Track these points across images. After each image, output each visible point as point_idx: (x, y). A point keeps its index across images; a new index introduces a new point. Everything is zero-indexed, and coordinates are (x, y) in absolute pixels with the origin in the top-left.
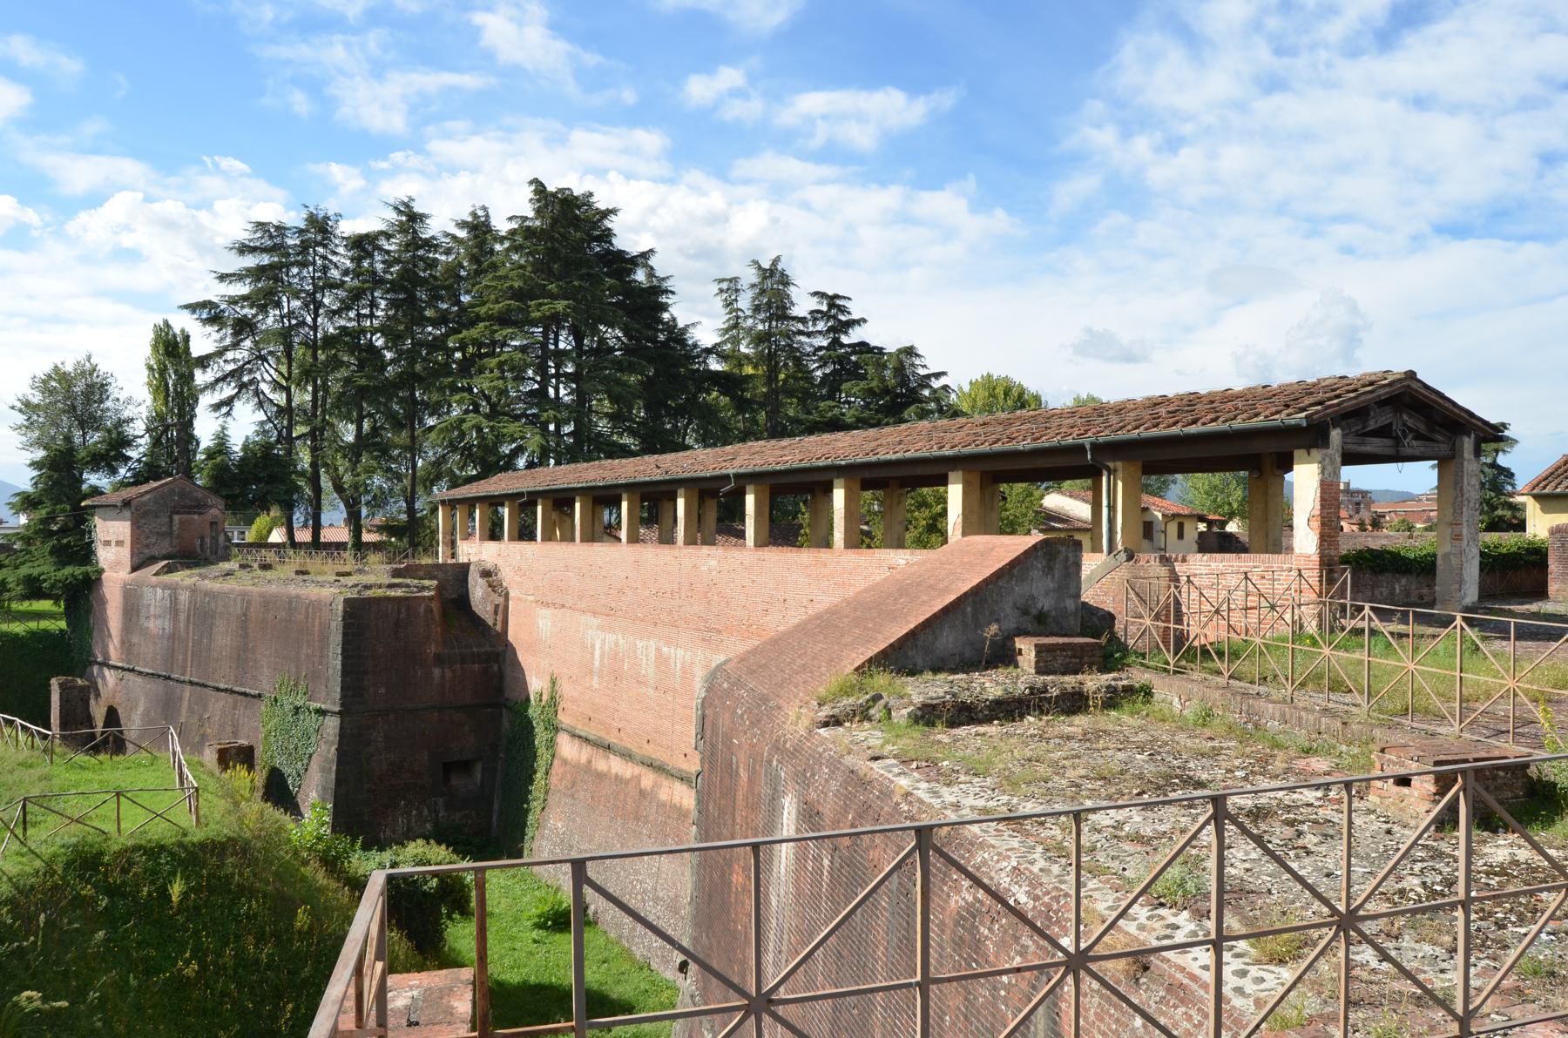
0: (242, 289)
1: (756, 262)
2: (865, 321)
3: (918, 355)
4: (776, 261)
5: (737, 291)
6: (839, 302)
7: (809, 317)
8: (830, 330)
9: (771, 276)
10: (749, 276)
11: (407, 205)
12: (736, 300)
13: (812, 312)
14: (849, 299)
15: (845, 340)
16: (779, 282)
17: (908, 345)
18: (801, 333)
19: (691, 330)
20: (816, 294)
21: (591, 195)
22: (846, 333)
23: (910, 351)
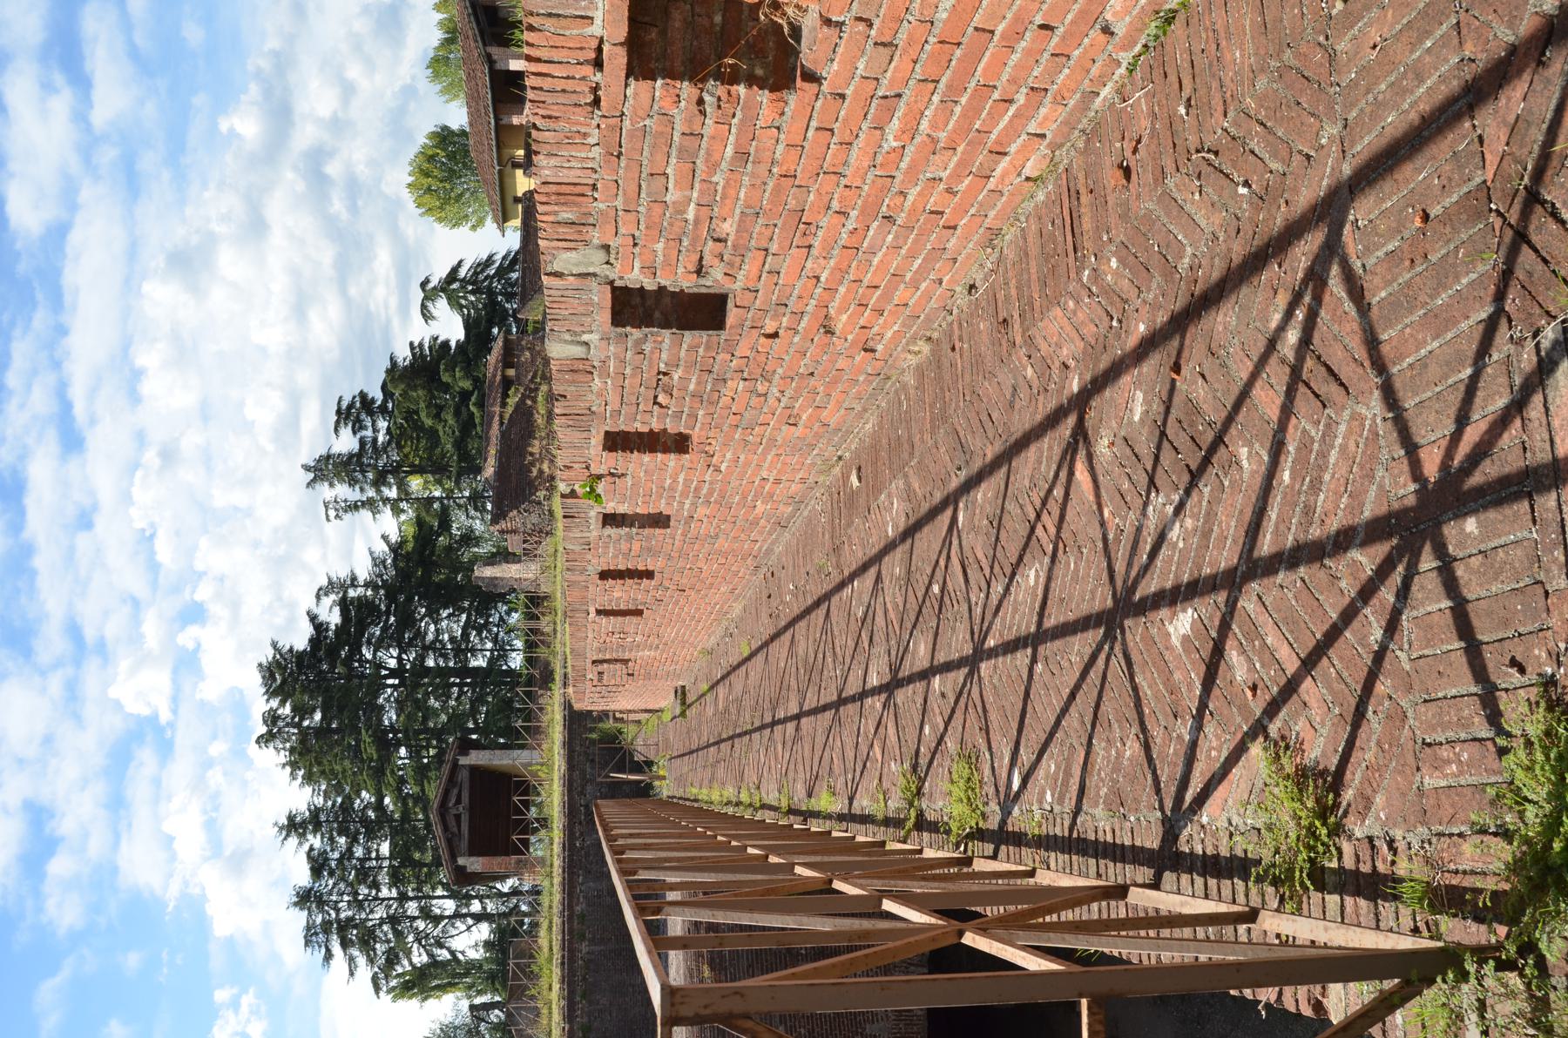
0: (361, 960)
1: (309, 485)
4: (307, 468)
6: (344, 407)
7: (358, 436)
8: (371, 413)
9: (321, 470)
10: (326, 492)
11: (281, 828)
12: (346, 501)
13: (354, 433)
16: (327, 464)
18: (375, 440)
19: (376, 555)
20: (336, 430)
21: (260, 665)
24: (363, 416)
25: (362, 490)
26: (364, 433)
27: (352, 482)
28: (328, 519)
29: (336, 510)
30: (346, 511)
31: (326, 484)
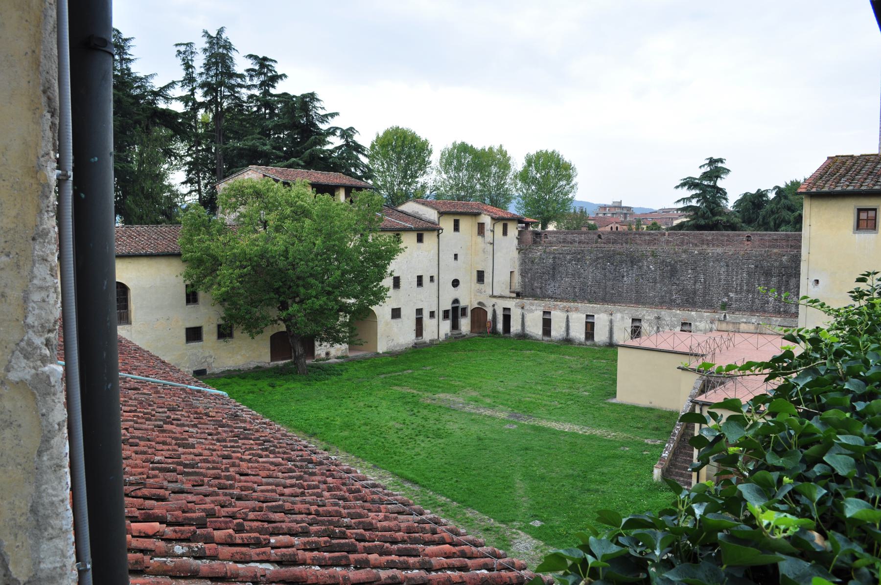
2: (285, 76)
3: (318, 100)
4: (220, 31)
5: (192, 53)
7: (246, 73)
8: (263, 84)
10: (201, 43)
12: (192, 60)
13: (248, 70)
14: (276, 62)
15: (272, 91)
16: (224, 47)
17: (310, 92)
18: (241, 86)
19: (150, 80)
20: (250, 56)
22: (273, 87)
23: (312, 97)
24: (262, 78)
25: (201, 74)
26: (248, 79)
27: (208, 66)
28: (177, 45)
29: (185, 52)
30: (183, 60)
31: (207, 45)
